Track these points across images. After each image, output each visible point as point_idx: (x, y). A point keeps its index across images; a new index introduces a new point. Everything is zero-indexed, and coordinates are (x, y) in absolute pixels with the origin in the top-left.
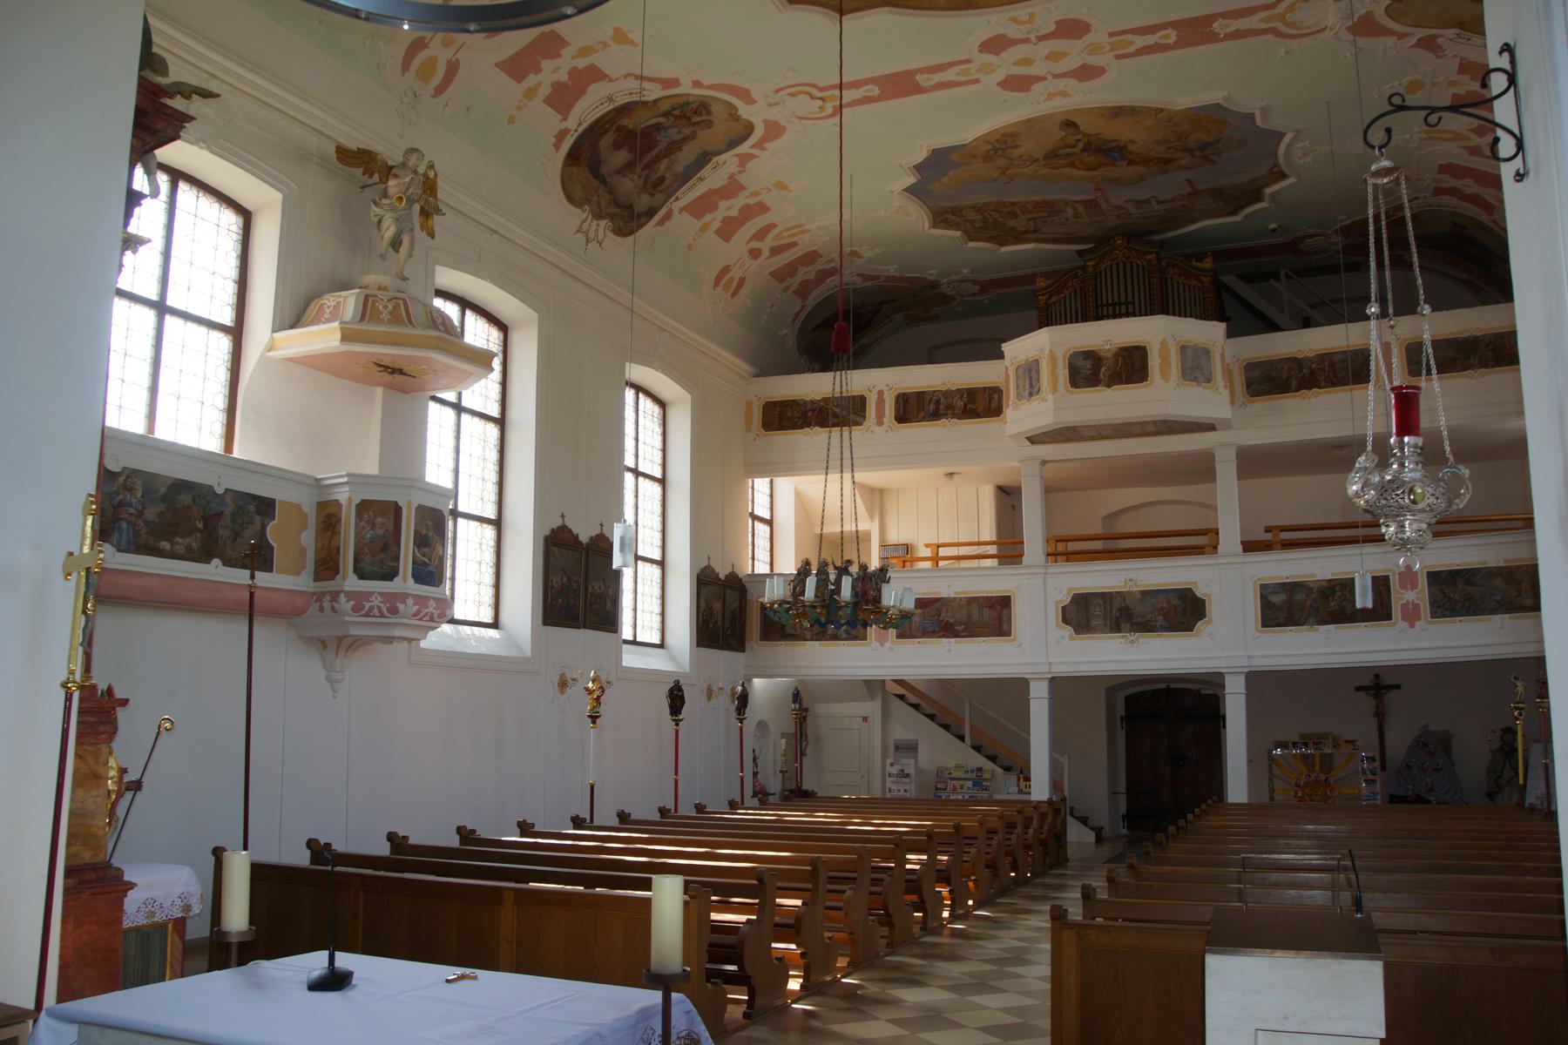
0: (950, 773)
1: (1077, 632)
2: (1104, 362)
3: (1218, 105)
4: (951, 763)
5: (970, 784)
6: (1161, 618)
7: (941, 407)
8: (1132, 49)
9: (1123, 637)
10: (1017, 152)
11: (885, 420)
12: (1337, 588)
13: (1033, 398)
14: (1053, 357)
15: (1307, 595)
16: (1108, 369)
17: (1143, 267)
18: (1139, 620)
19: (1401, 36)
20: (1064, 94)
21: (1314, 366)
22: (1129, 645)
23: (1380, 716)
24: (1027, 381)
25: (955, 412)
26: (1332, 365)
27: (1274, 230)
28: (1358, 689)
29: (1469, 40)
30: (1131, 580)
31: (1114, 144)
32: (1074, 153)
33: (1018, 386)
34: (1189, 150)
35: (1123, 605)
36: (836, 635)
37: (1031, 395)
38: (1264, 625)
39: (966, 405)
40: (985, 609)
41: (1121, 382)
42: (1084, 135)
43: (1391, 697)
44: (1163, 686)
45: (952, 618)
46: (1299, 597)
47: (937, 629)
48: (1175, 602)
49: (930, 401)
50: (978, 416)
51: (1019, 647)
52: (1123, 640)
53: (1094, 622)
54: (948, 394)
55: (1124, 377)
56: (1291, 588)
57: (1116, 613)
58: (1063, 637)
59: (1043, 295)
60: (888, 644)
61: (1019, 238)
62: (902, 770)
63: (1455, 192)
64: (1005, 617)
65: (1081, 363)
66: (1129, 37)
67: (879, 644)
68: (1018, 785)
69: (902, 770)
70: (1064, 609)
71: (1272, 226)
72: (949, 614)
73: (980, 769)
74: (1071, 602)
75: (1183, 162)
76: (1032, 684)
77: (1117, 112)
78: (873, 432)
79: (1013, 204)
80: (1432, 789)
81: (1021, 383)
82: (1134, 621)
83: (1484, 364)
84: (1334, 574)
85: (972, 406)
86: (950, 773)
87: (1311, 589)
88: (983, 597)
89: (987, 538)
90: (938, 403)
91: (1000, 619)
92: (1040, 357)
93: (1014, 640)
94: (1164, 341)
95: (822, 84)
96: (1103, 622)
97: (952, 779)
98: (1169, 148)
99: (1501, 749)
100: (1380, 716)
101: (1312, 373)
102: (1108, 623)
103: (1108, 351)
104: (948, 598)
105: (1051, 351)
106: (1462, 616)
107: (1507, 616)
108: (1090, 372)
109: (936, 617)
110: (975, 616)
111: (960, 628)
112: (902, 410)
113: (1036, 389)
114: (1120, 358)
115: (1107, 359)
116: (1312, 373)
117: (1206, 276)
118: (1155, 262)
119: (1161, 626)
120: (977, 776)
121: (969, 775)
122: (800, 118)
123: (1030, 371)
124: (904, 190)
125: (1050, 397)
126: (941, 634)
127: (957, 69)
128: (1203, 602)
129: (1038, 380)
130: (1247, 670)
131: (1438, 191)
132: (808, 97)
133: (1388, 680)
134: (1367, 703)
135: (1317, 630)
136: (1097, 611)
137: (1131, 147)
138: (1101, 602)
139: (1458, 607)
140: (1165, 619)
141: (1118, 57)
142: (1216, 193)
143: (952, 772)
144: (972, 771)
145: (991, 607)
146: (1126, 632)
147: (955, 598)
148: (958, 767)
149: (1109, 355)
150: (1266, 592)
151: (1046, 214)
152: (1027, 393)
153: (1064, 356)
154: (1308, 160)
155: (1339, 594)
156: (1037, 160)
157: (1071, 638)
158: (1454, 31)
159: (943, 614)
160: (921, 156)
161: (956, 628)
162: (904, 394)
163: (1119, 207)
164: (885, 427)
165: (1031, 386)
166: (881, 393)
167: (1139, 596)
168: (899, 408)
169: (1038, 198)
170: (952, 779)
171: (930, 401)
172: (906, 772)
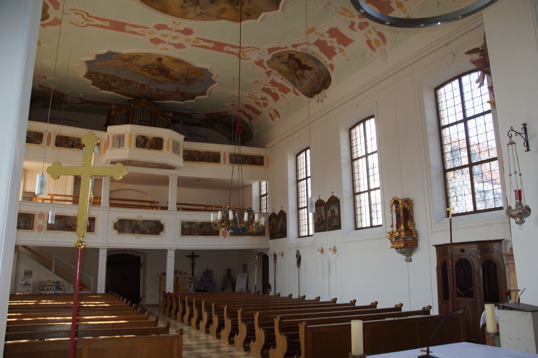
0: (45, 284)
1: (119, 233)
2: (149, 141)
3: (207, 69)
4: (45, 279)
5: (54, 287)
6: (149, 230)
7: (75, 144)
8: (198, 44)
9: (135, 235)
10: (136, 62)
11: (51, 144)
12: (205, 225)
13: (119, 148)
14: (131, 135)
15: (196, 226)
16: (150, 143)
17: (150, 110)
18: (141, 230)
19: (265, 68)
20: (167, 50)
21: (204, 155)
22: (137, 238)
23: (193, 265)
24: (118, 142)
25: (80, 146)
26: (209, 155)
27: (189, 109)
28: (187, 256)
29: (278, 75)
30: (139, 216)
31: (168, 70)
32: (153, 68)
33: (113, 143)
34: (186, 79)
35: (136, 224)
37: (119, 146)
38: (182, 235)
41: (153, 149)
42: (161, 64)
43: (197, 260)
44: (122, 253)
45: (71, 223)
46: (193, 226)
47: (64, 228)
48: (154, 225)
49: (71, 140)
52: (135, 237)
53: (126, 230)
55: (154, 147)
56: (191, 223)
57: (133, 227)
58: (114, 234)
59: (114, 111)
60: (43, 232)
61: (109, 90)
62: (27, 283)
63: (244, 113)
65: (140, 139)
66: (201, 41)
67: (38, 232)
69: (27, 283)
70: (115, 224)
71: (189, 108)
72: (70, 222)
73: (58, 282)
74: (118, 222)
75: (182, 82)
76: (100, 251)
77: (177, 61)
79: (119, 78)
80: (208, 288)
81: (115, 142)
82: (140, 230)
83: (249, 164)
84: (203, 220)
87: (197, 224)
89: (69, 194)
90: (74, 142)
92: (125, 135)
93: (95, 234)
94: (169, 138)
95: (90, 14)
96: (128, 230)
97: (46, 286)
98: (182, 76)
99: (227, 275)
100: (193, 265)
101: (203, 157)
102: (130, 230)
103: (150, 137)
105: (130, 133)
106: (238, 236)
107: (249, 237)
108: (143, 143)
109: (65, 223)
113: (122, 145)
114: (154, 141)
115: (149, 140)
116: (203, 157)
117: (170, 119)
118: (154, 110)
119: (148, 232)
120: (57, 284)
121: (54, 284)
122: (71, 22)
123: (120, 138)
124: (86, 61)
125: (128, 149)
126: (66, 229)
127: (142, 29)
128: (163, 225)
129: (123, 142)
130: (176, 249)
131: (240, 111)
132: (82, 16)
133: (196, 254)
134: (189, 261)
135: (198, 237)
136: (127, 226)
137: (171, 73)
138: (128, 223)
139: (237, 233)
140: (150, 230)
141: (192, 45)
142: (183, 94)
143: (46, 283)
144: (55, 283)
146: (137, 234)
147: (73, 217)
148: (49, 281)
149: (151, 139)
150: (183, 224)
151: (126, 84)
152: (117, 146)
153: (135, 136)
154: (215, 92)
155: (205, 226)
156: (139, 67)
157: (117, 235)
158: (277, 72)
160: (104, 51)
161: (73, 228)
163: (152, 89)
164: (50, 147)
165: (120, 143)
166: (50, 134)
167: (142, 221)
168: (58, 140)
169: (128, 78)
170: (46, 286)
171: (71, 140)
172: (28, 283)
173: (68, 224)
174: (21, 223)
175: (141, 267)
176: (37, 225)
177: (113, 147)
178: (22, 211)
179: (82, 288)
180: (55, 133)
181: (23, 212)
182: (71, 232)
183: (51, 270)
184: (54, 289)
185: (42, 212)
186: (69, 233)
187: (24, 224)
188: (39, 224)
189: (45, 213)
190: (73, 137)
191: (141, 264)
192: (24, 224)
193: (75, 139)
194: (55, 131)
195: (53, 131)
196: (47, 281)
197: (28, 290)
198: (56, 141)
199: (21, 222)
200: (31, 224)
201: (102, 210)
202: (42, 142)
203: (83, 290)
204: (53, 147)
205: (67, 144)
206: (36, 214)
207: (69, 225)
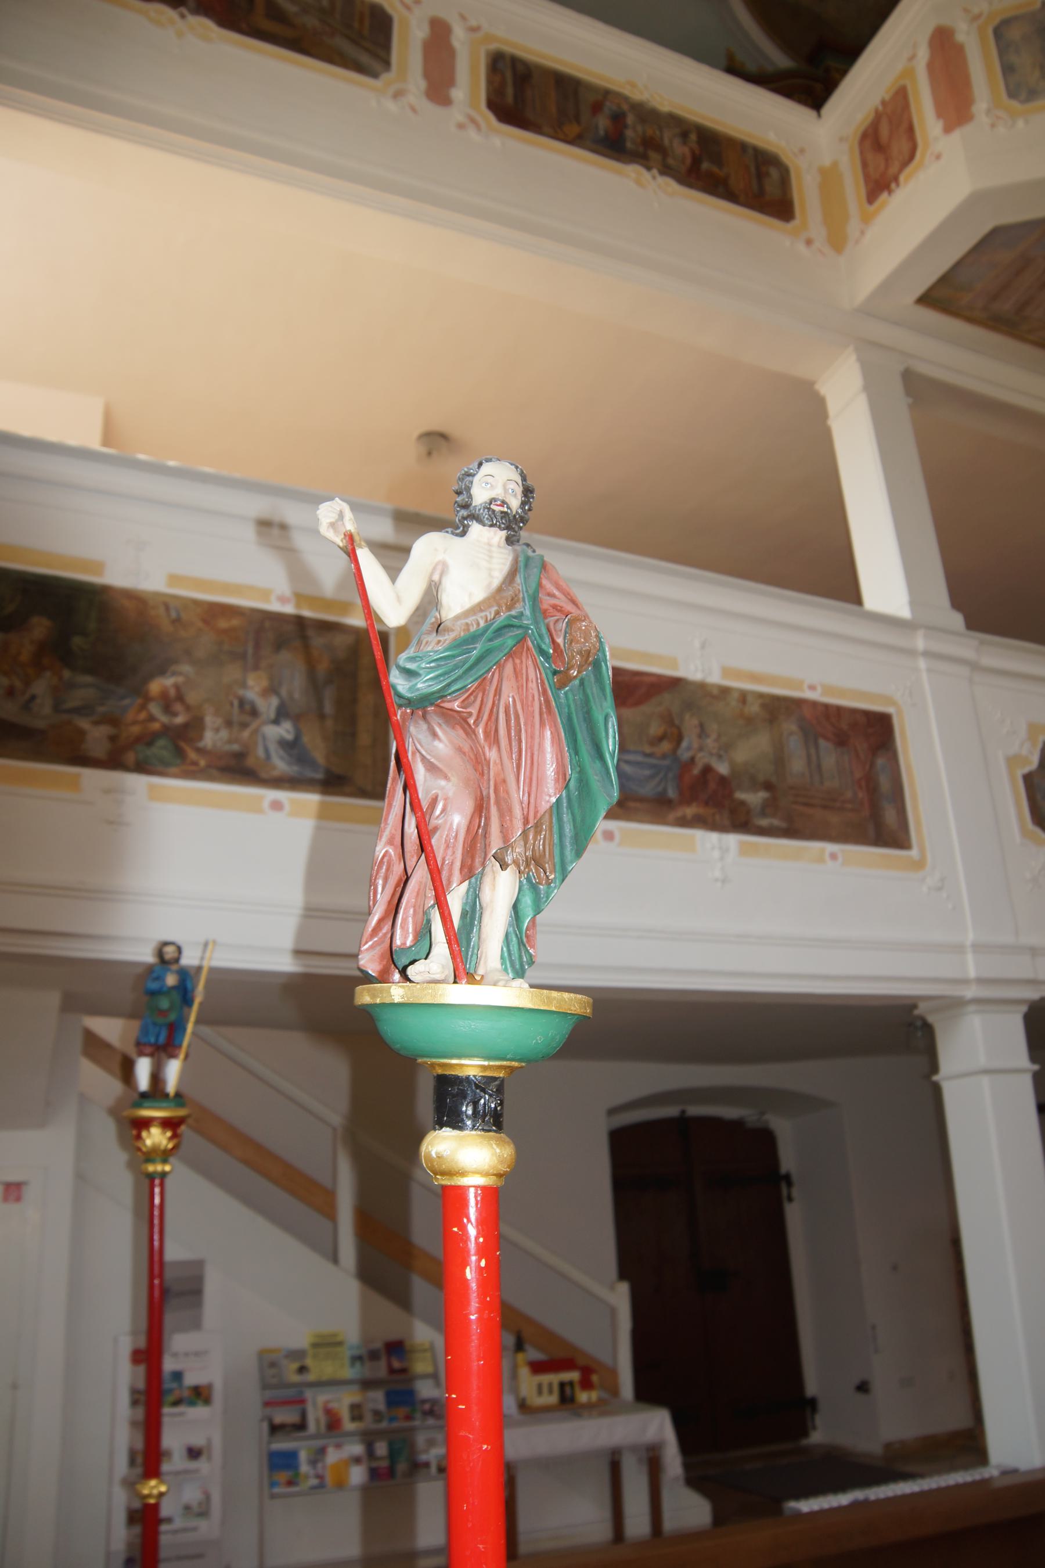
0: (302, 1369)
11: (459, 94)
25: (670, 161)
36: (240, 756)
39: (696, 161)
40: (822, 743)
44: (671, 1111)
47: (672, 793)
50: (731, 196)
51: (940, 889)
54: (646, 114)
64: (884, 783)
72: (710, 742)
78: (414, 110)
85: (715, 169)
86: (302, 1369)
88: (814, 704)
90: (618, 118)
91: (870, 784)
93: (919, 865)
104: (702, 686)
109: (666, 746)
110: (797, 765)
111: (754, 798)
112: (510, 91)
120: (392, 1371)
126: (690, 811)
143: (309, 1362)
145: (841, 741)
147: (725, 691)
159: (690, 742)
161: (740, 795)
162: (515, 61)
164: (457, 113)
171: (597, 108)
173: (692, 760)
174: (254, 713)
175: (790, 1199)
177: (1012, 94)
179: (571, 1383)
180: (474, 30)
182: (732, 840)
183: (335, 1259)
184: (377, 1415)
186: (724, 851)
187: (285, 730)
190: (607, 93)
191: (788, 1179)
192: (285, 730)
193: (625, 107)
194: (474, 23)
195: (463, 18)
196: (315, 1345)
197: (197, 1440)
198: (490, 82)
199: (261, 704)
200: (364, 738)
201: (927, 654)
202: (387, 64)
203: (583, 1397)
204: (474, 114)
205: (577, 119)
207: (707, 770)
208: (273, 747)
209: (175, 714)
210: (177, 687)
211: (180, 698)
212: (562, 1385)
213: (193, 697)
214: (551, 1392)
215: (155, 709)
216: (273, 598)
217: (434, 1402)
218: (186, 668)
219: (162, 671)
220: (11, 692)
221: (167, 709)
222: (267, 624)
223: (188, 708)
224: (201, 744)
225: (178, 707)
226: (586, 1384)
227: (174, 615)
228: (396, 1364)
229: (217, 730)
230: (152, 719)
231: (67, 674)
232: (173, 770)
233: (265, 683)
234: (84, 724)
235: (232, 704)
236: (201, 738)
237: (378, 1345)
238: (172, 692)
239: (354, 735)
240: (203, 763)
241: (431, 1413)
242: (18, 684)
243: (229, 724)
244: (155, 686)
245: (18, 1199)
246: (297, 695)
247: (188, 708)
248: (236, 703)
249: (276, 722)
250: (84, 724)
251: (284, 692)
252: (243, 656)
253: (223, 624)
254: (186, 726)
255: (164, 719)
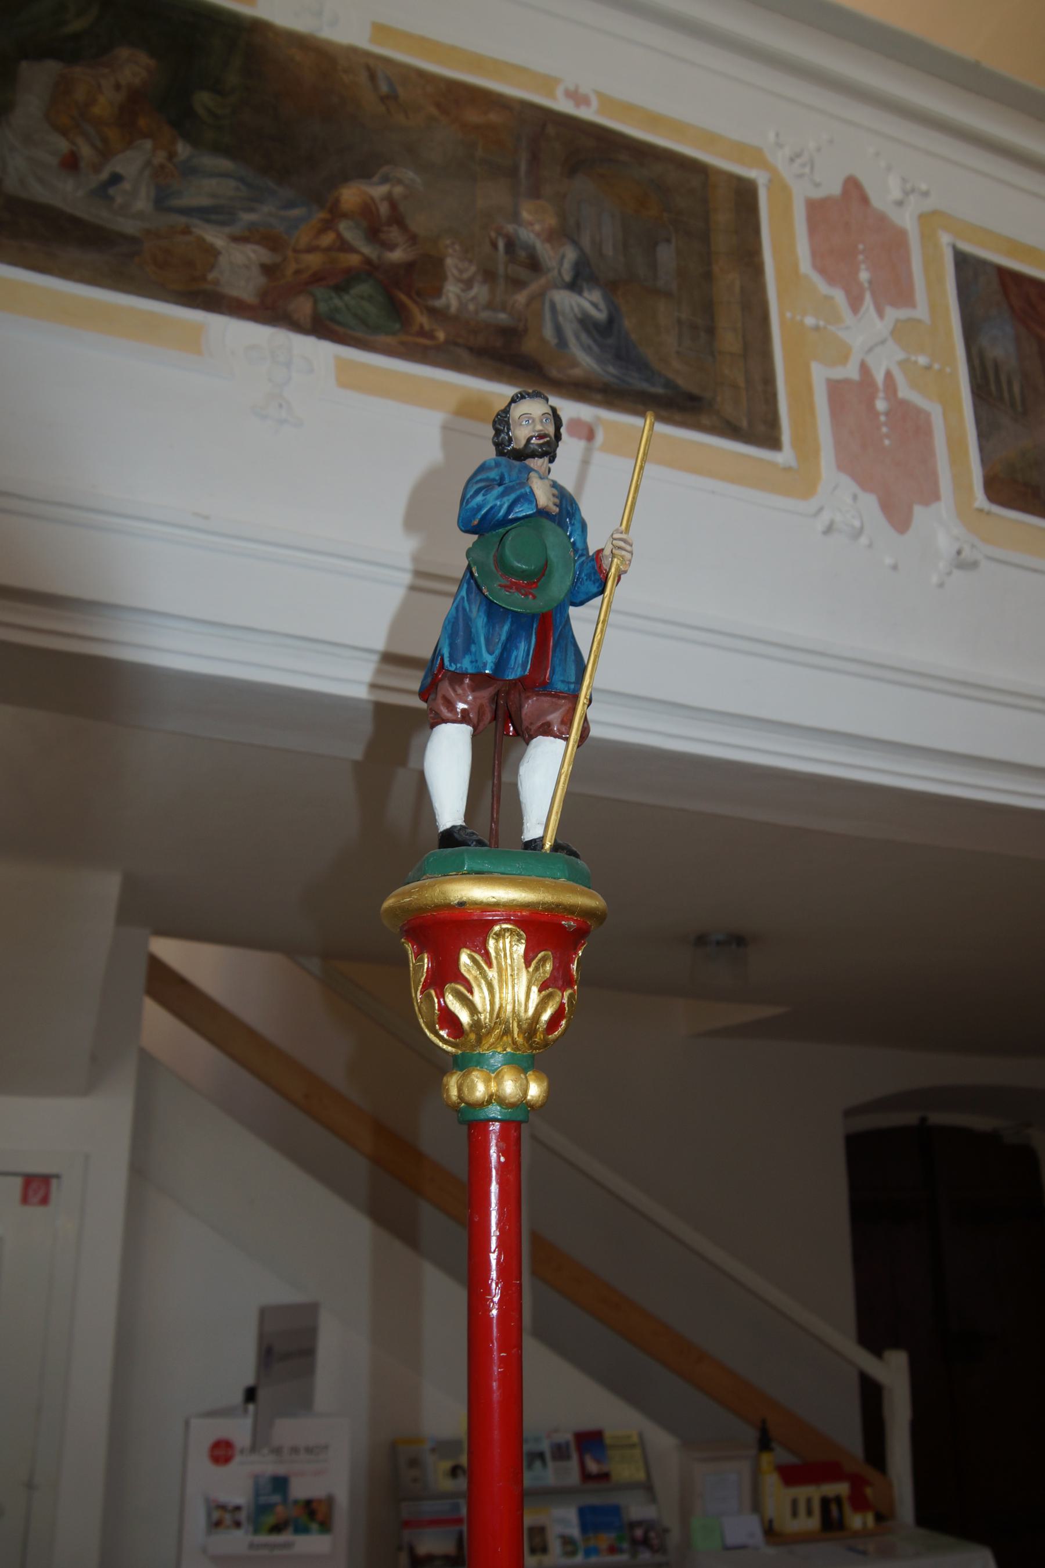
36: (511, 334)
62: (280, 1484)
68: (757, 1507)
69: (280, 1484)
120: (586, 1477)
144: (560, 1452)
172: (301, 1490)
174: (534, 265)
176: (820, 374)
178: (548, 83)
179: (838, 1500)
181: (563, 105)
185: (853, 187)
188: (851, 371)
189: (907, 220)
199: (545, 252)
200: (729, 341)
203: (856, 1521)
206: (781, 189)
208: (570, 330)
209: (392, 247)
210: (389, 198)
211: (397, 219)
212: (825, 1502)
213: (419, 222)
214: (809, 1513)
215: (349, 231)
216: (560, 92)
217: (649, 1525)
218: (409, 175)
219: (365, 171)
220: (71, 163)
221: (374, 233)
222: (551, 130)
223: (413, 239)
224: (439, 303)
225: (394, 234)
226: (860, 1503)
227: (384, 88)
228: (593, 1467)
229: (468, 284)
230: (344, 246)
231: (183, 149)
232: (383, 339)
233: (552, 221)
234: (215, 237)
235: (494, 245)
236: (438, 292)
237: (566, 1437)
238: (384, 209)
239: (711, 331)
240: (441, 336)
241: (645, 1542)
242: (86, 151)
243: (489, 276)
244: (350, 195)
245: (45, 1201)
246: (609, 251)
247: (413, 239)
248: (501, 245)
249: (574, 286)
250: (215, 237)
251: (586, 241)
252: (513, 172)
253: (473, 116)
254: (409, 267)
255: (368, 250)
